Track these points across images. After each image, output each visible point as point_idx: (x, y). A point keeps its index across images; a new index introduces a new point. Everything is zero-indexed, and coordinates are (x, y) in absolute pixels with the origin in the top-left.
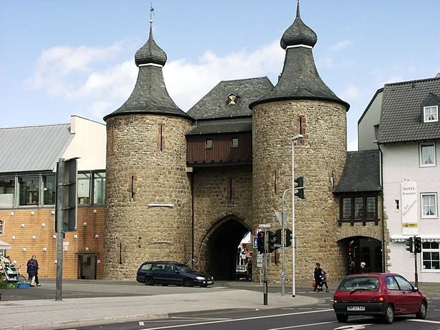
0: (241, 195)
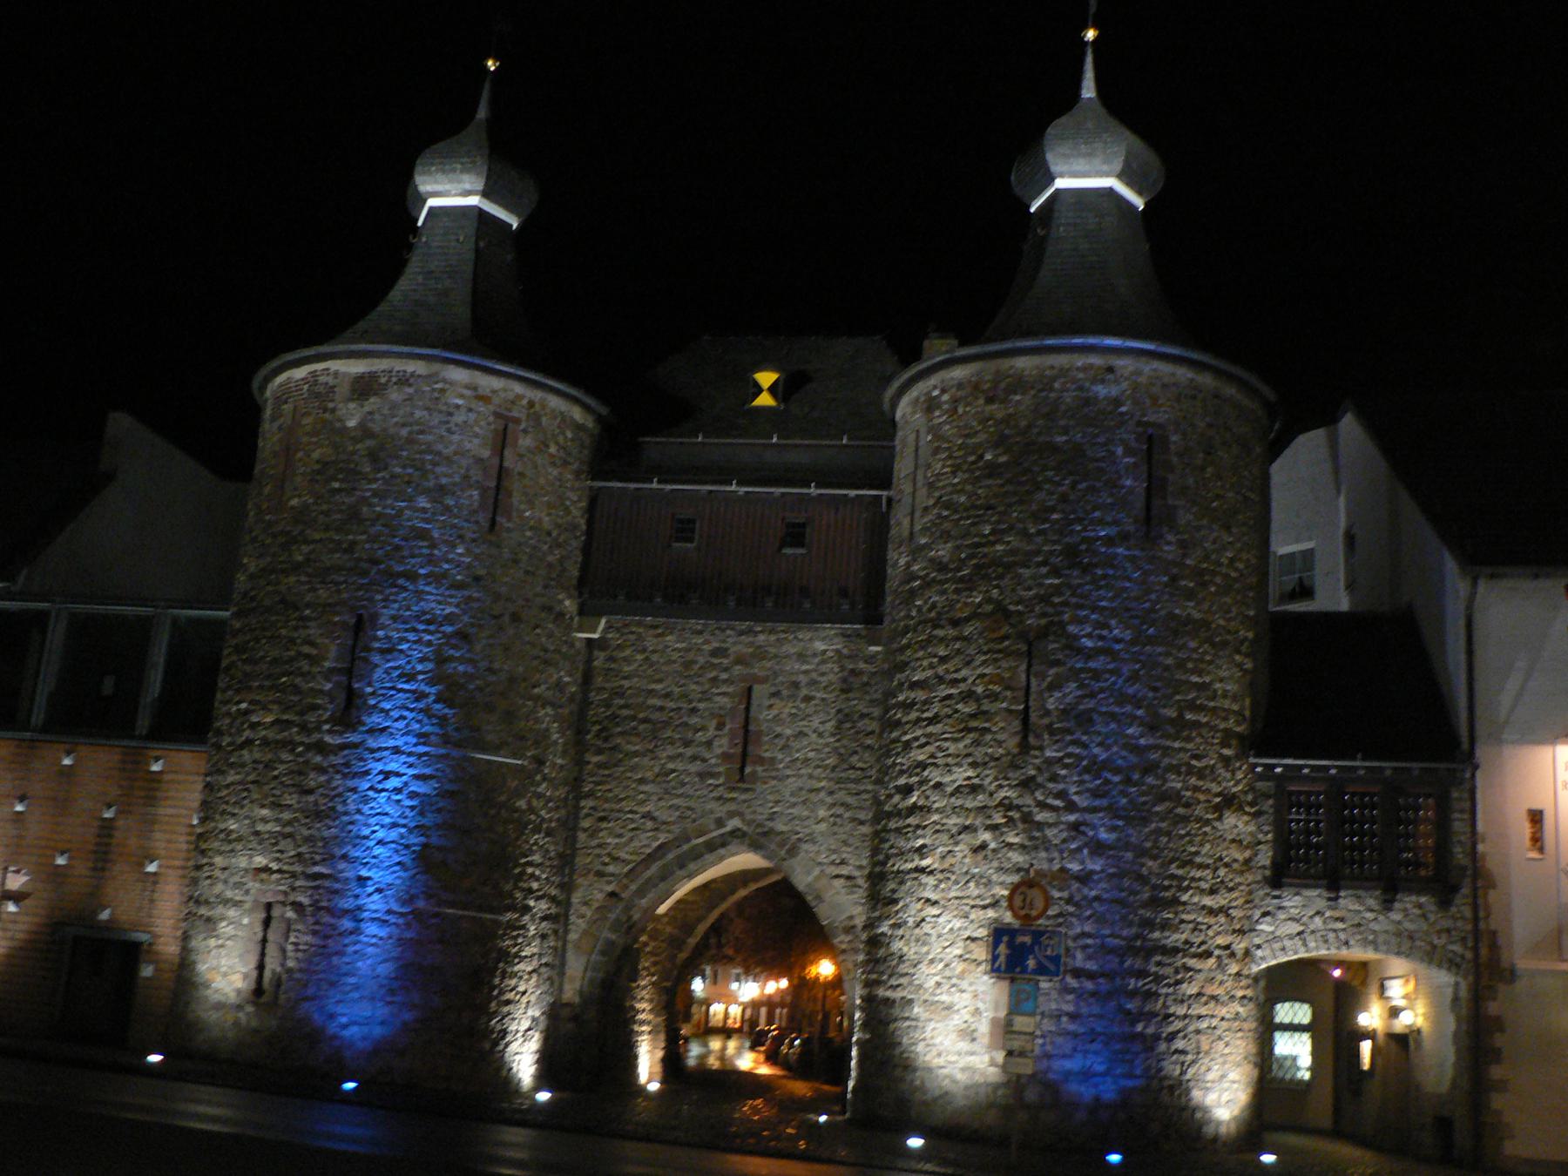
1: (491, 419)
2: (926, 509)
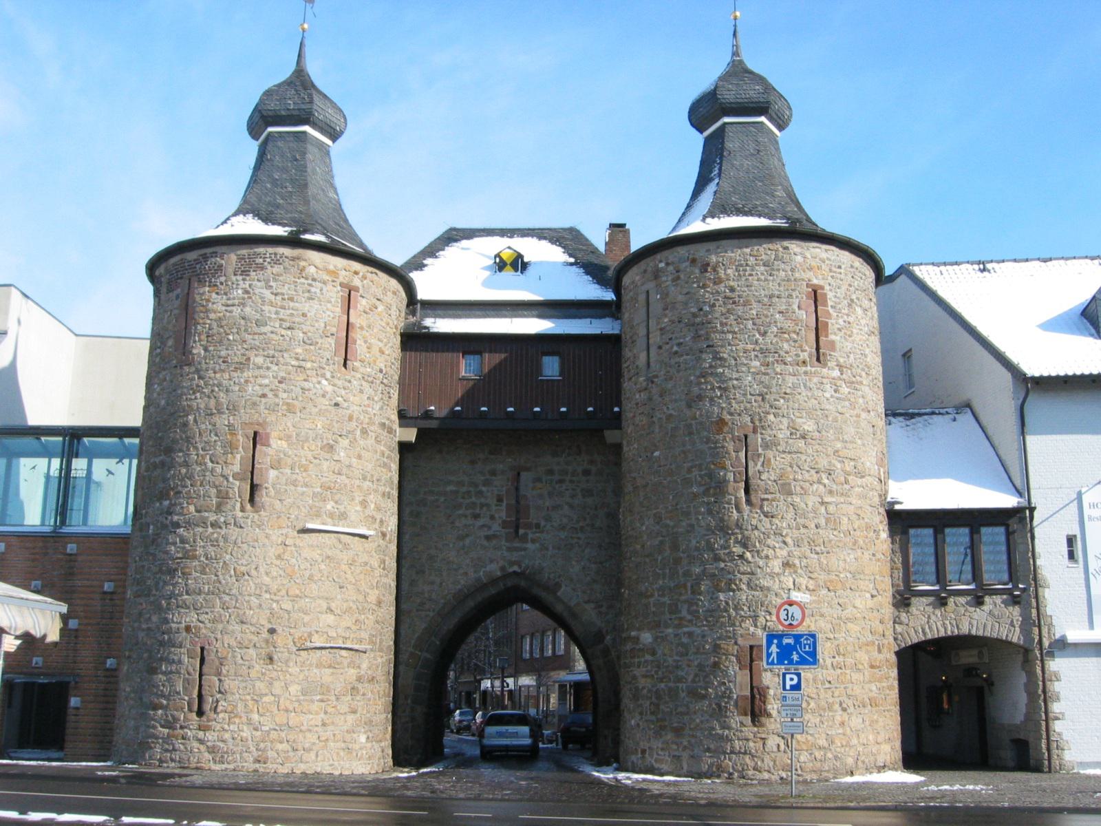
0: (548, 519)
1: (339, 288)
2: (660, 347)
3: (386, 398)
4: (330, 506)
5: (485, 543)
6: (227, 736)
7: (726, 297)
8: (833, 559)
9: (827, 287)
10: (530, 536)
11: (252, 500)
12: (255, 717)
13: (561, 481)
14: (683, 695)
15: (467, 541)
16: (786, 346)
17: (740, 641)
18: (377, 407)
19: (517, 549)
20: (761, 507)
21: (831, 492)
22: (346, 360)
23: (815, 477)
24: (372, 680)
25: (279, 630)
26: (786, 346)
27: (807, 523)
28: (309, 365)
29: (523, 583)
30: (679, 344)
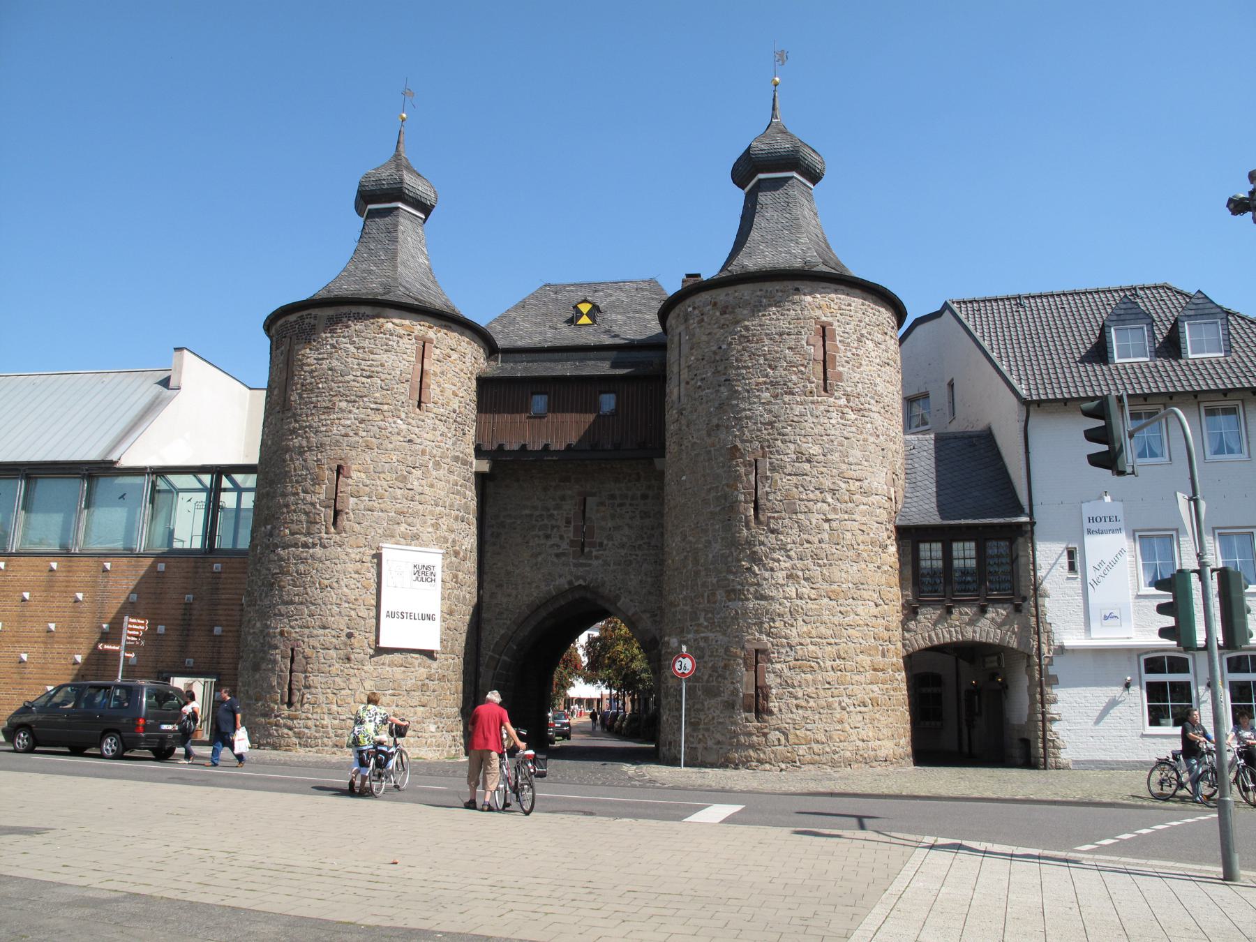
3: (460, 433)
4: (403, 527)
5: (555, 560)
6: (310, 723)
7: (742, 336)
8: (835, 569)
9: (836, 324)
10: (594, 553)
11: (335, 523)
12: (334, 707)
13: (621, 505)
14: (700, 693)
15: (540, 559)
16: (794, 377)
17: (747, 645)
18: (450, 442)
19: (582, 565)
20: (768, 525)
21: (835, 510)
22: (420, 402)
23: (820, 496)
24: (442, 678)
25: (356, 633)
26: (794, 377)
27: (811, 538)
28: (386, 407)
29: (589, 595)
30: (703, 379)
